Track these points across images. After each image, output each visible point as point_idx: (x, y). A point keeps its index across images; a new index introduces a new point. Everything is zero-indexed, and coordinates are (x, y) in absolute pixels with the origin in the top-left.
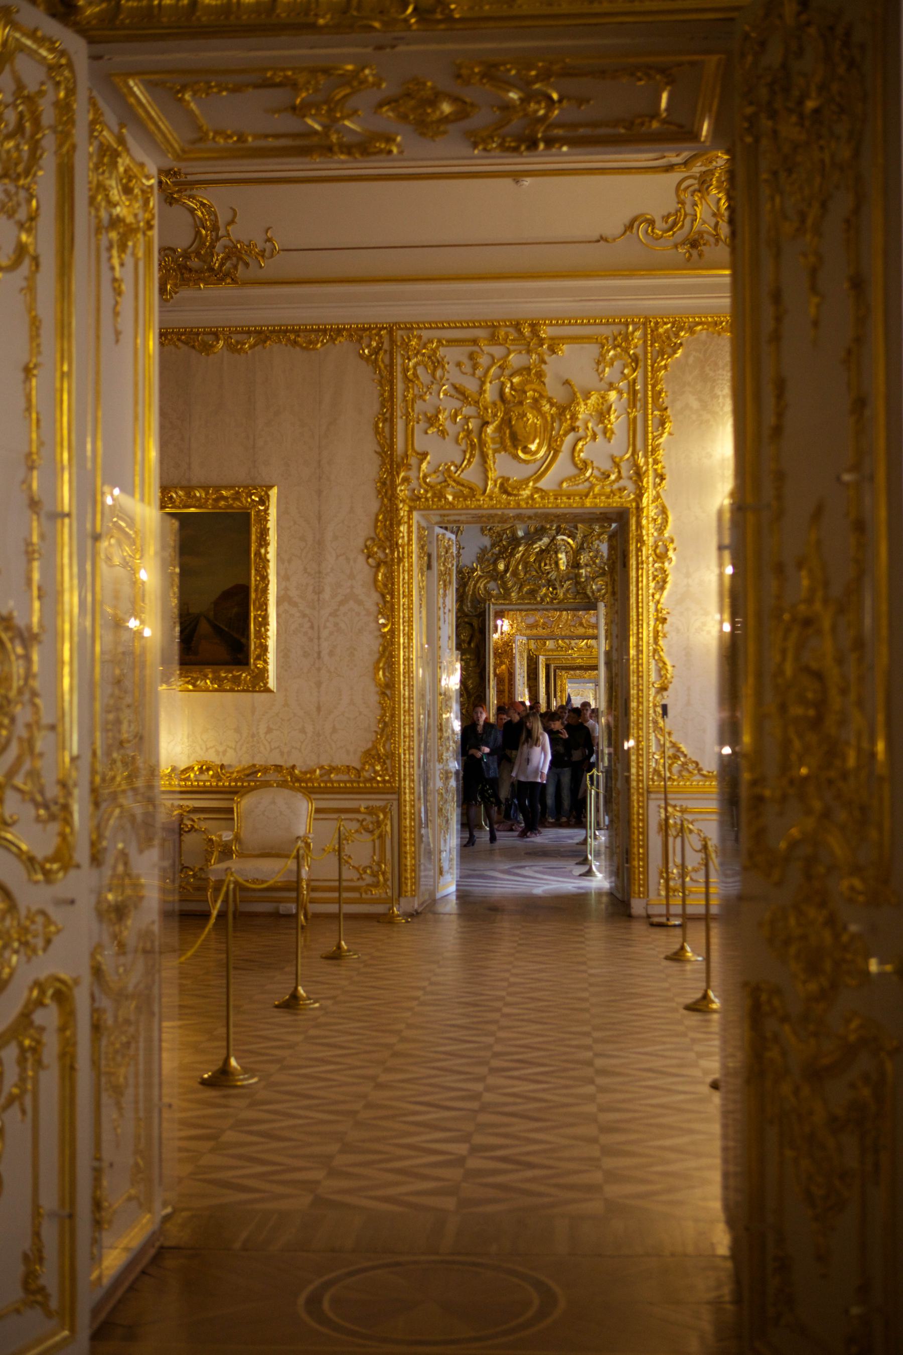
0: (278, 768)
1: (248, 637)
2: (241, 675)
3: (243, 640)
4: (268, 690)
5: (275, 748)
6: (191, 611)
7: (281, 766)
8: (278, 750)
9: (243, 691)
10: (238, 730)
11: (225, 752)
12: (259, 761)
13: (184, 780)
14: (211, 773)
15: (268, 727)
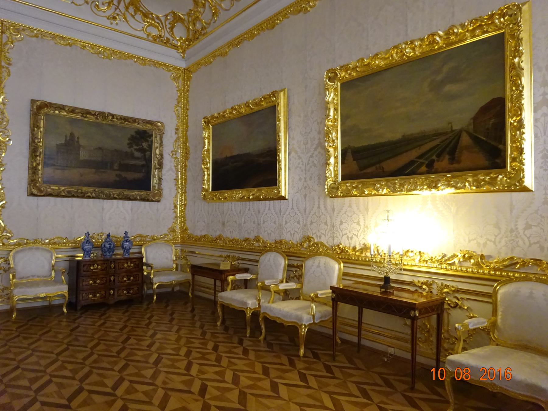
0: (537, 262)
1: (505, 144)
2: (497, 177)
3: (501, 146)
4: (526, 189)
5: (534, 243)
6: (454, 129)
7: (540, 261)
8: (538, 245)
9: (499, 191)
10: (497, 226)
11: (485, 245)
12: (517, 254)
13: (450, 264)
14: (472, 261)
15: (527, 223)
